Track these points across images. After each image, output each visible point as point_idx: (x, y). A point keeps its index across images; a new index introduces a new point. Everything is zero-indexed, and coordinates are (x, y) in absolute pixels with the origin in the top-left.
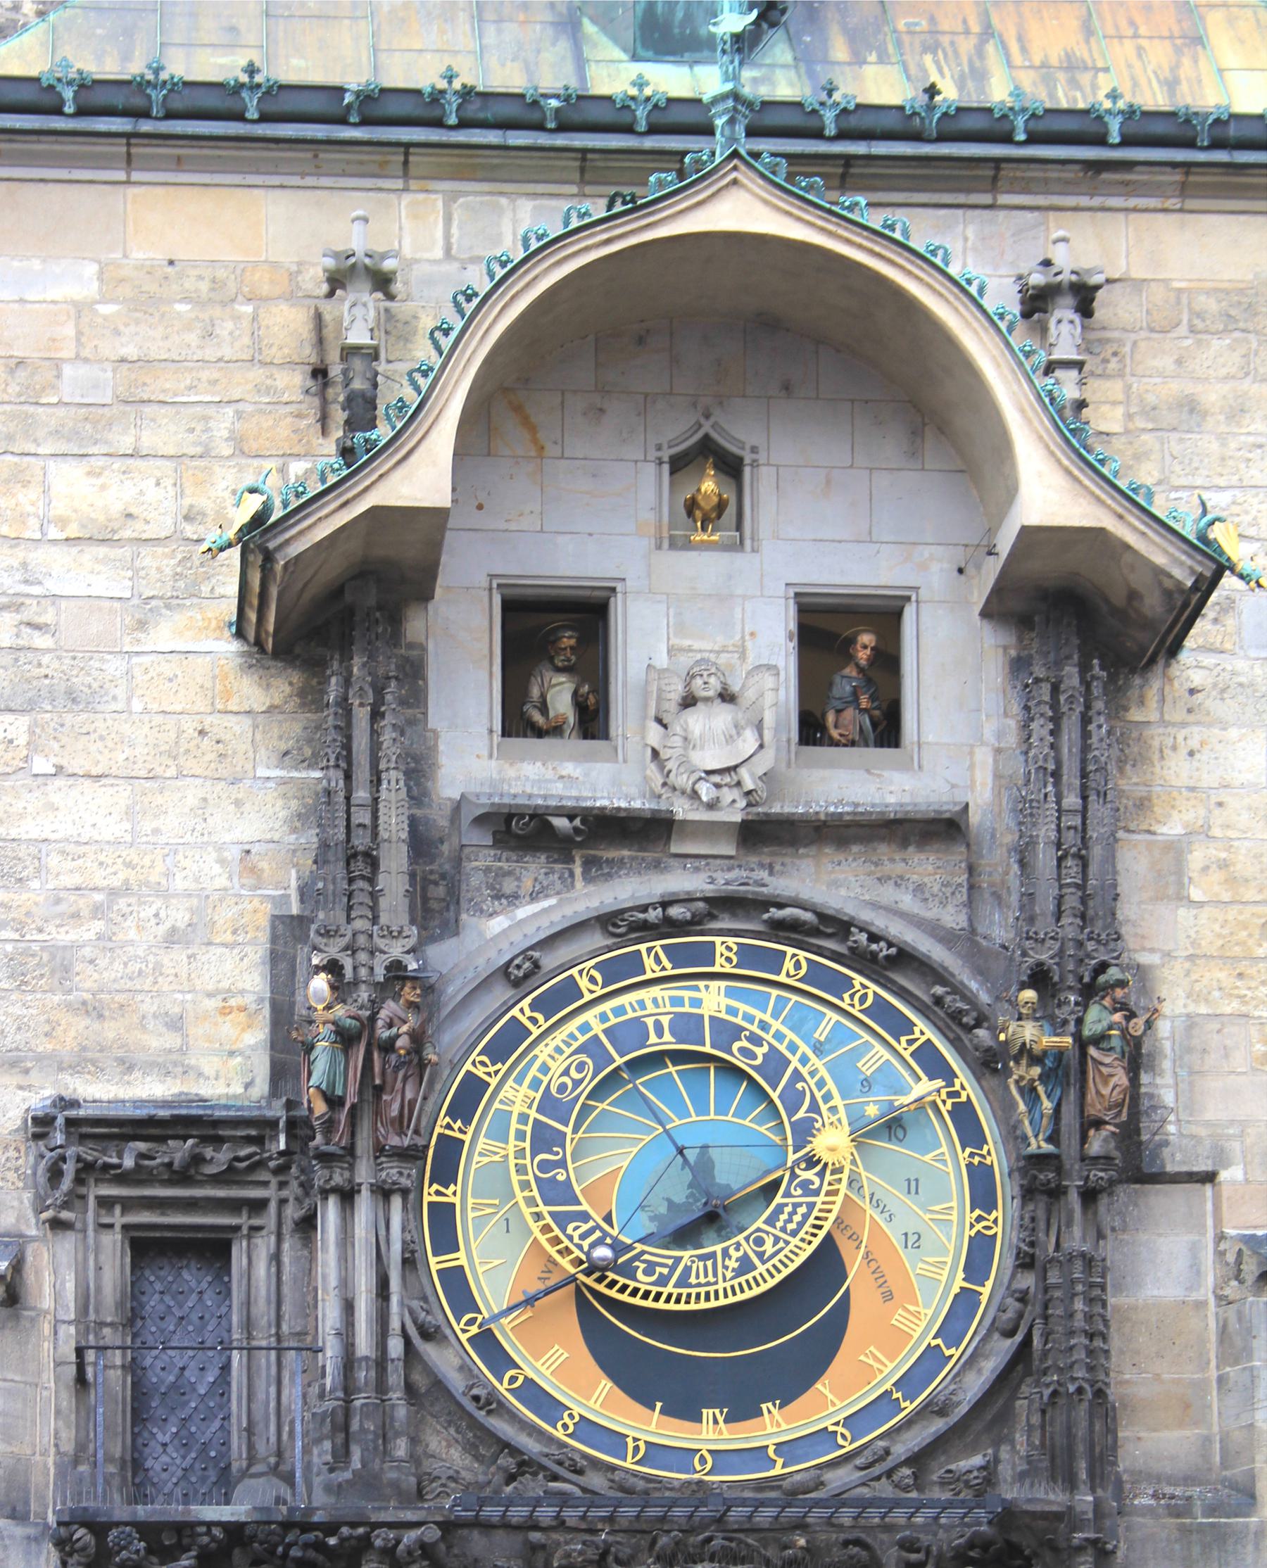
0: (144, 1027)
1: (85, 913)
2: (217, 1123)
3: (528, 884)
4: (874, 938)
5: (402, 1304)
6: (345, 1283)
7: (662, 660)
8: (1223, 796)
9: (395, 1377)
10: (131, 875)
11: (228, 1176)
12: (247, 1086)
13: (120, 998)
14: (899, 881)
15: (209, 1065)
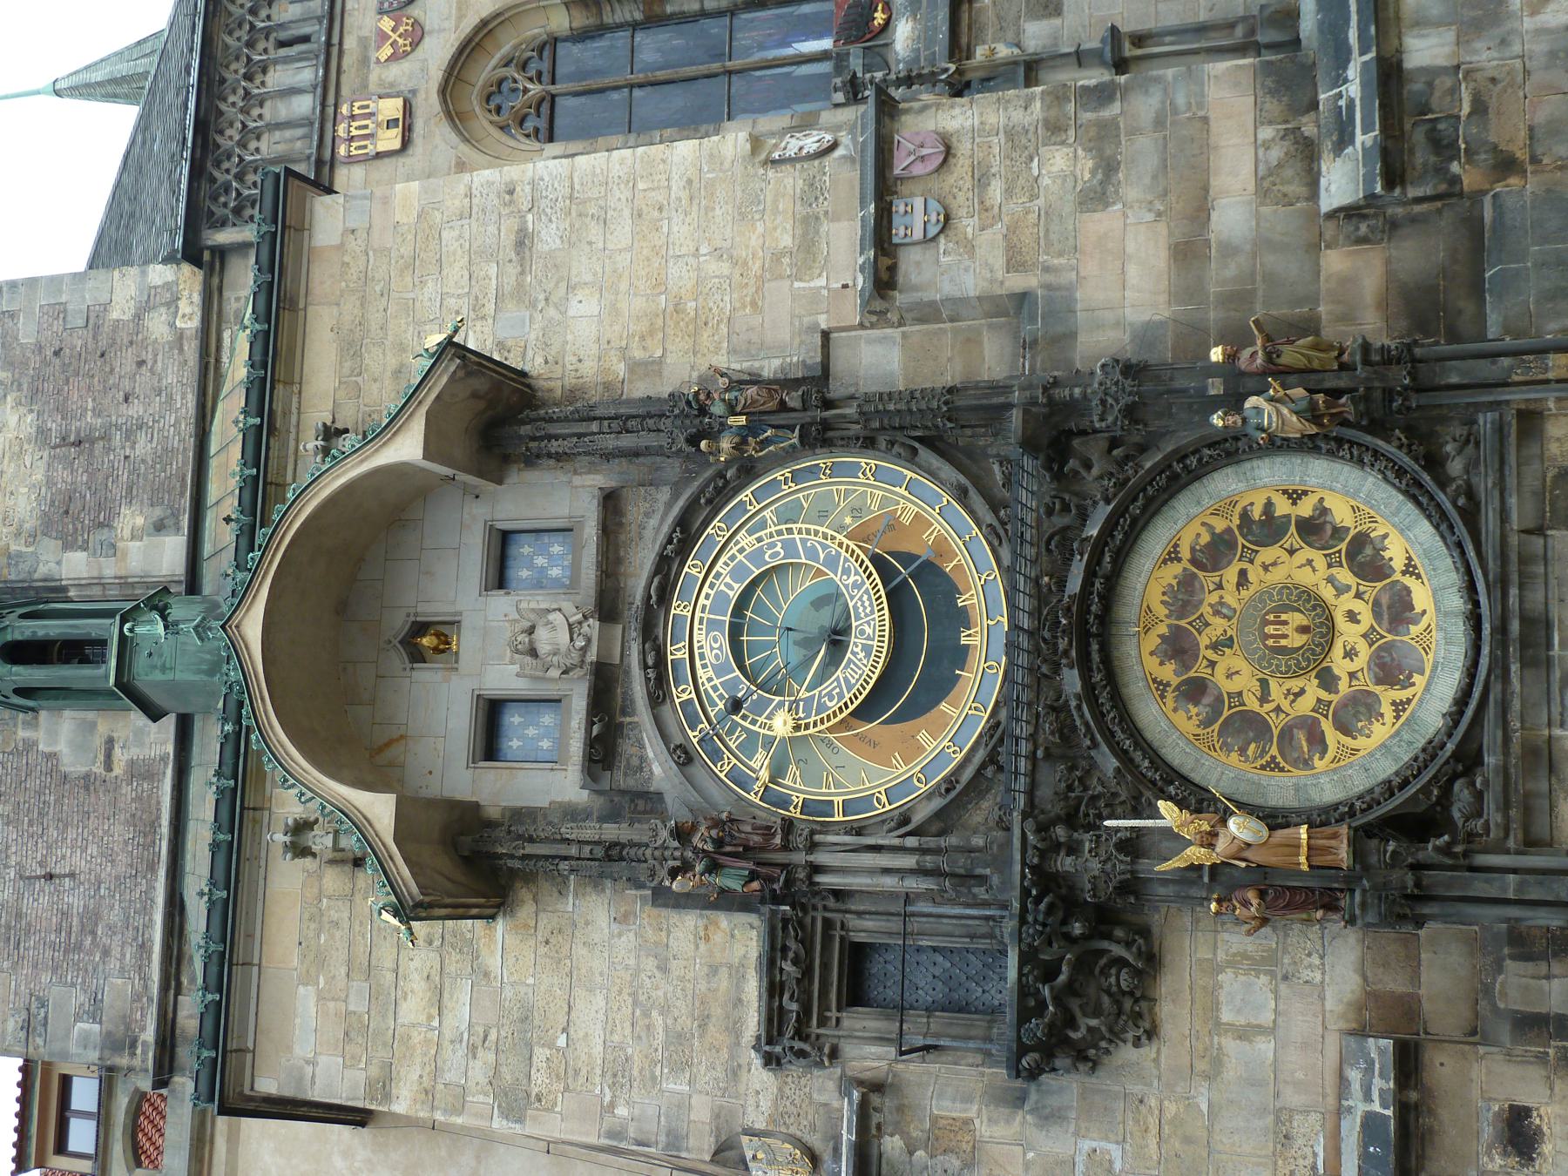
0: (716, 990)
1: (647, 1021)
2: (772, 947)
3: (634, 750)
4: (670, 541)
5: (883, 838)
6: (872, 871)
7: (516, 668)
8: (603, 341)
9: (930, 842)
10: (626, 991)
11: (807, 943)
12: (752, 927)
13: (697, 1004)
14: (642, 527)
15: (739, 951)
